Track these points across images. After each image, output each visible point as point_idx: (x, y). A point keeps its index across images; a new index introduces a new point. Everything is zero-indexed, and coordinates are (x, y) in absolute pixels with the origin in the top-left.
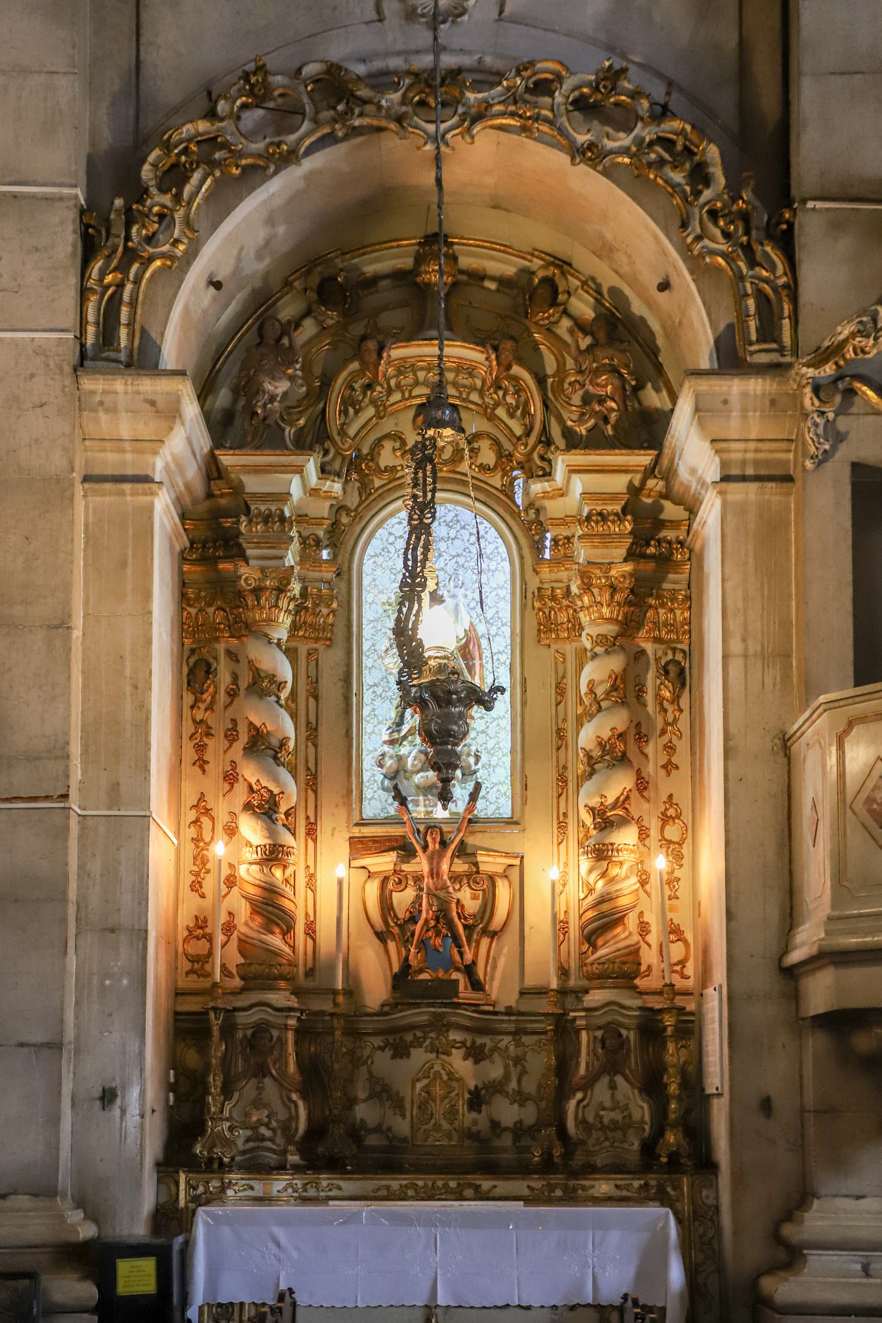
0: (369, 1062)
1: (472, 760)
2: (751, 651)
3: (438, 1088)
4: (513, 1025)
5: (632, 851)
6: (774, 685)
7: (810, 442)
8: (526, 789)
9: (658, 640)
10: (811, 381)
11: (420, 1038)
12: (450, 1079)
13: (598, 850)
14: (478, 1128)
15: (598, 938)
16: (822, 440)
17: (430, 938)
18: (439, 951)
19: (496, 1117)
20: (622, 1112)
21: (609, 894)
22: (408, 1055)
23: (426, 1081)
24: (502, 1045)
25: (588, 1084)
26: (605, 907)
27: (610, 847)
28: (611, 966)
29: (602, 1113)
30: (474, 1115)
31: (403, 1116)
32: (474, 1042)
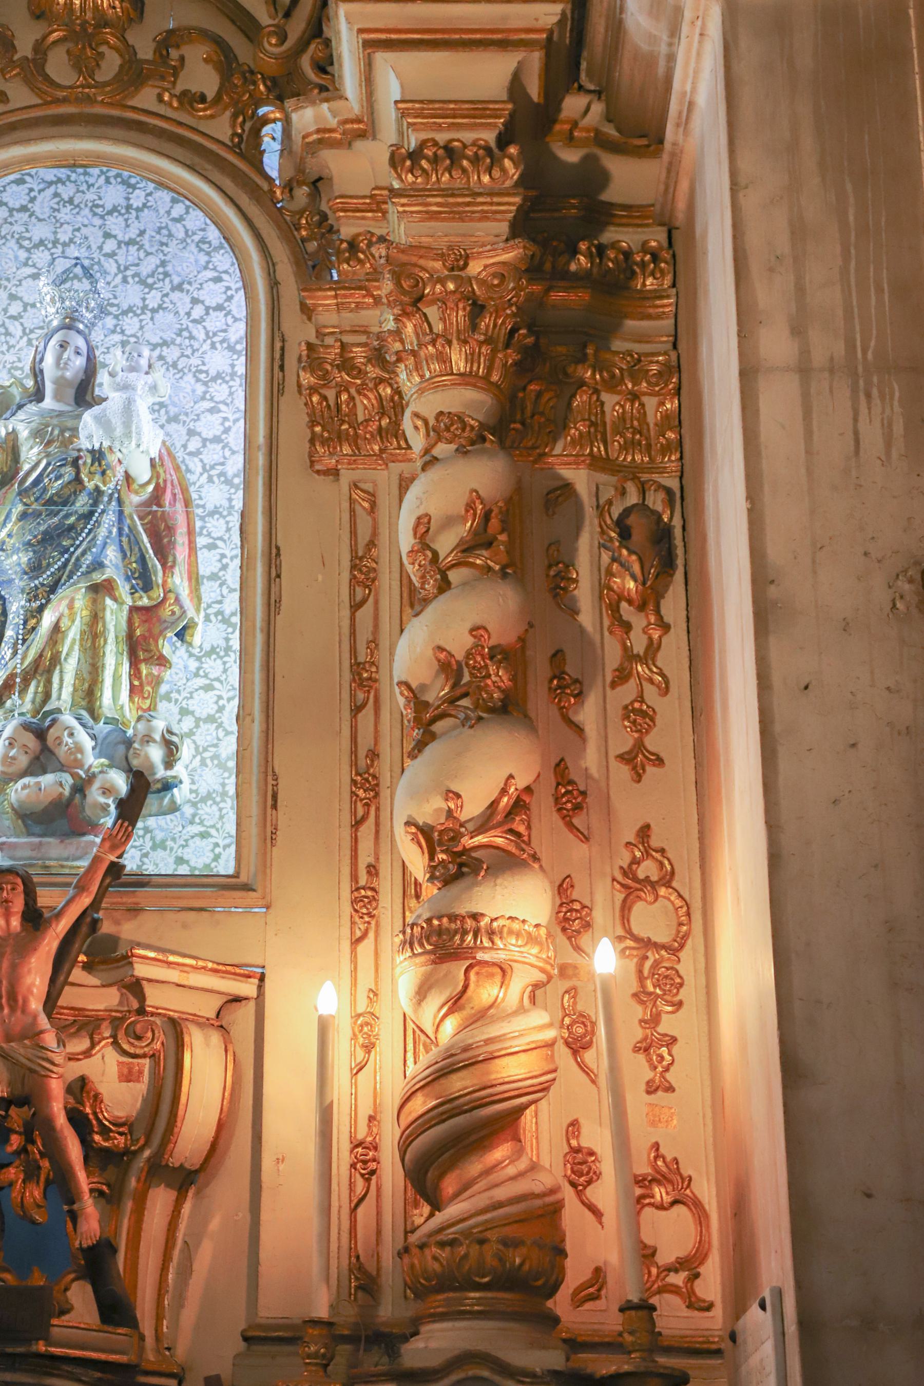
1: (156, 754)
5: (531, 939)
8: (275, 806)
9: (598, 463)
13: (440, 932)
15: (442, 1176)
17: (11, 1184)
18: (33, 1222)
21: (466, 1049)
26: (459, 1083)
27: (470, 923)
28: (475, 1250)
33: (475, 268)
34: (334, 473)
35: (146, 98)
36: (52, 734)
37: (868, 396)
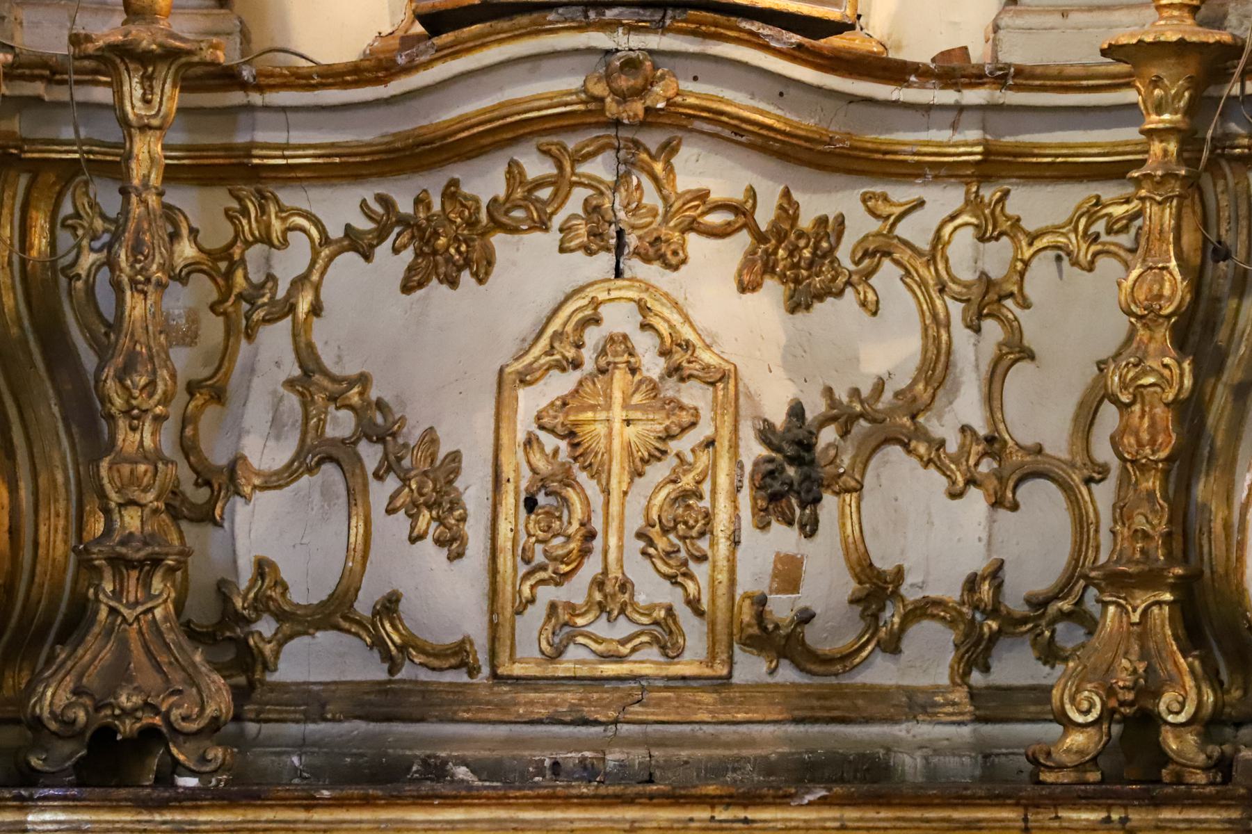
0: (304, 306)
3: (618, 414)
4: (974, 135)
11: (540, 184)
12: (676, 372)
22: (482, 267)
23: (560, 384)
24: (915, 230)
30: (784, 538)
31: (452, 544)
32: (788, 209)
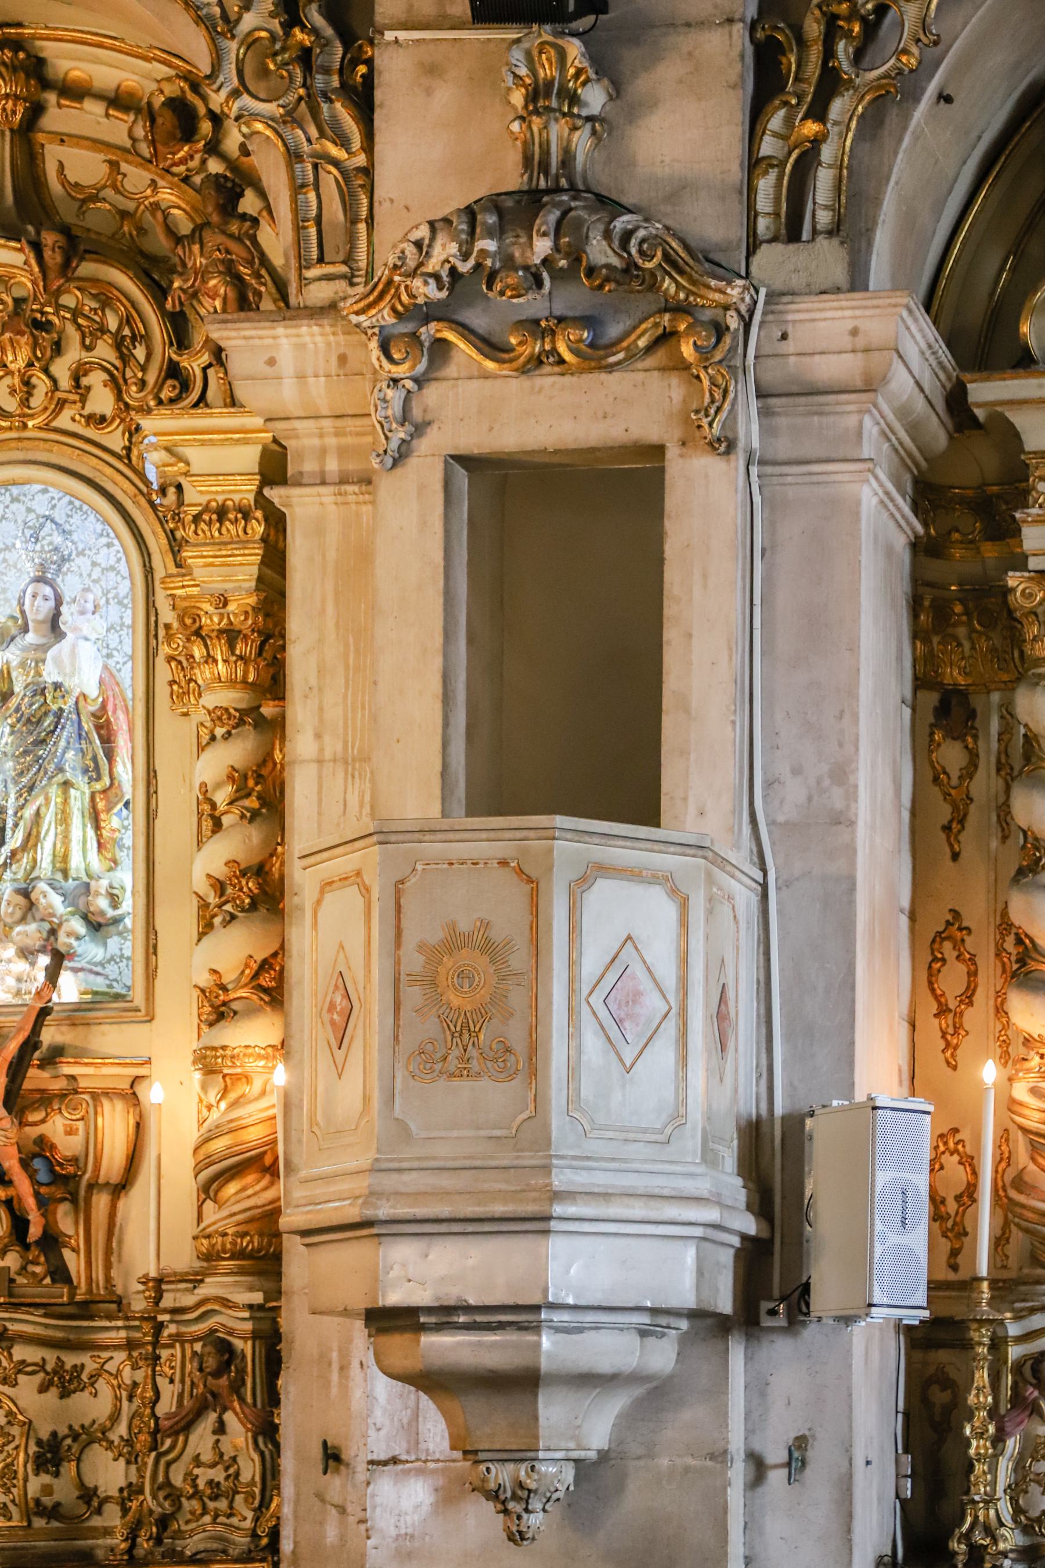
2: (328, 755)
5: (260, 1057)
6: (361, 806)
7: (378, 426)
10: (376, 330)
14: (56, 1497)
16: (394, 426)
19: (90, 1483)
20: (227, 1469)
25: (185, 1425)
28: (220, 1239)
29: (196, 1471)
30: (46, 1479)
33: (232, 607)
34: (186, 714)
35: (64, 421)
36: (33, 896)
37: (353, 777)
